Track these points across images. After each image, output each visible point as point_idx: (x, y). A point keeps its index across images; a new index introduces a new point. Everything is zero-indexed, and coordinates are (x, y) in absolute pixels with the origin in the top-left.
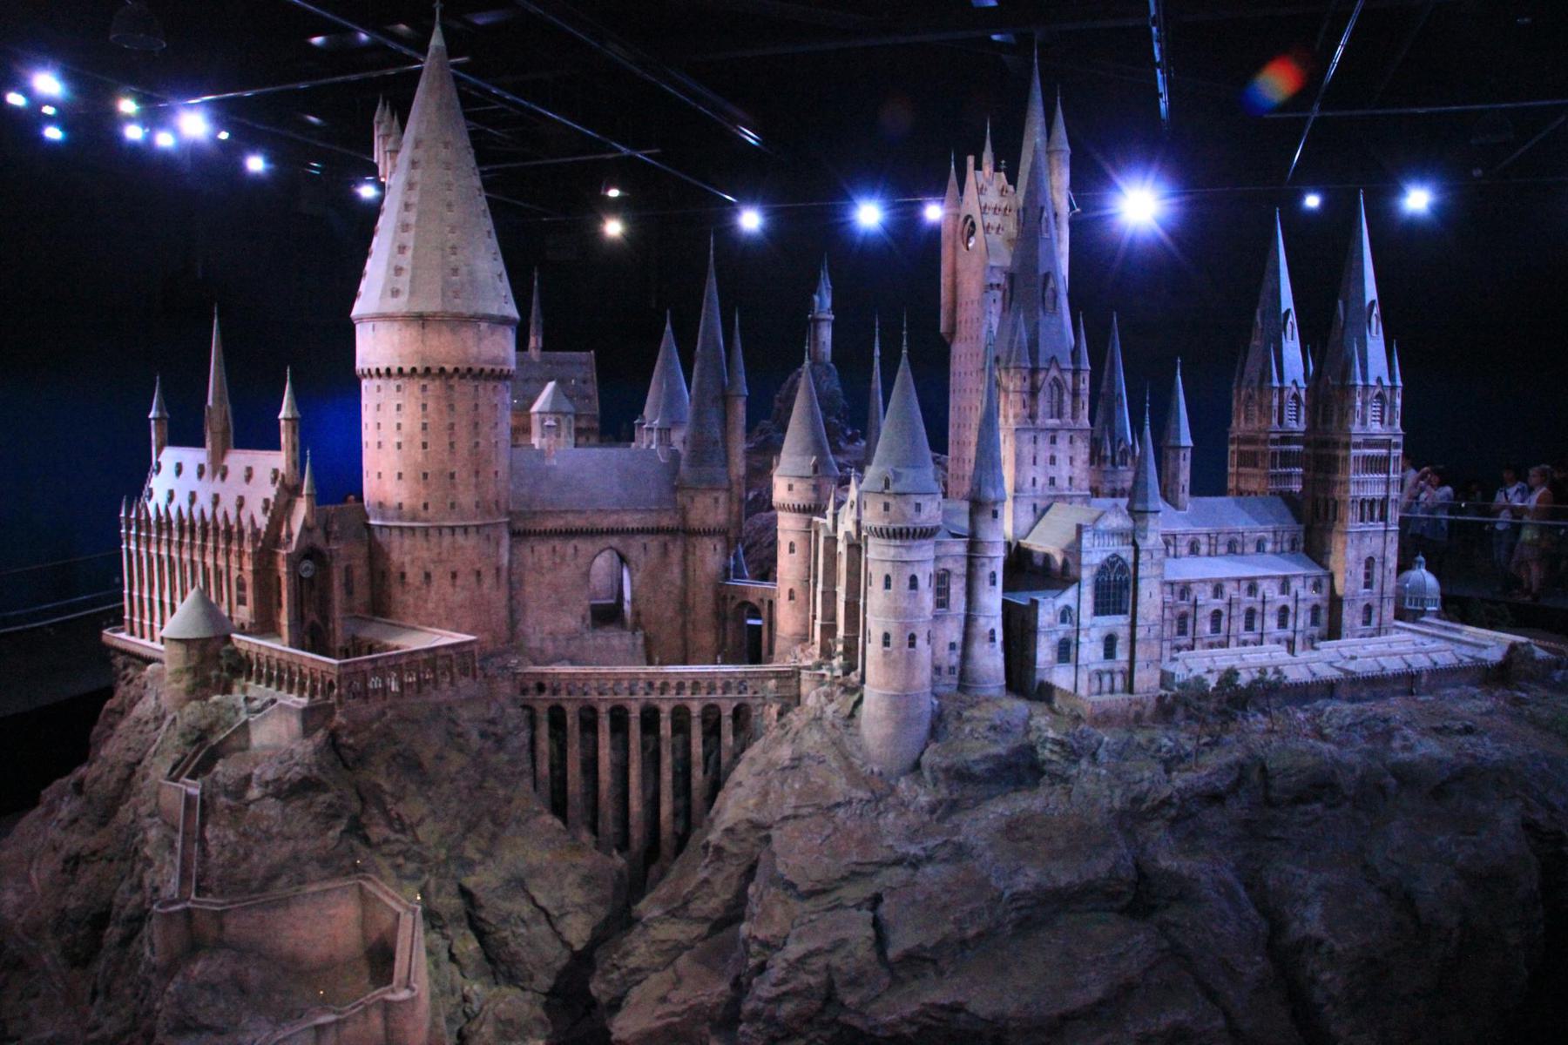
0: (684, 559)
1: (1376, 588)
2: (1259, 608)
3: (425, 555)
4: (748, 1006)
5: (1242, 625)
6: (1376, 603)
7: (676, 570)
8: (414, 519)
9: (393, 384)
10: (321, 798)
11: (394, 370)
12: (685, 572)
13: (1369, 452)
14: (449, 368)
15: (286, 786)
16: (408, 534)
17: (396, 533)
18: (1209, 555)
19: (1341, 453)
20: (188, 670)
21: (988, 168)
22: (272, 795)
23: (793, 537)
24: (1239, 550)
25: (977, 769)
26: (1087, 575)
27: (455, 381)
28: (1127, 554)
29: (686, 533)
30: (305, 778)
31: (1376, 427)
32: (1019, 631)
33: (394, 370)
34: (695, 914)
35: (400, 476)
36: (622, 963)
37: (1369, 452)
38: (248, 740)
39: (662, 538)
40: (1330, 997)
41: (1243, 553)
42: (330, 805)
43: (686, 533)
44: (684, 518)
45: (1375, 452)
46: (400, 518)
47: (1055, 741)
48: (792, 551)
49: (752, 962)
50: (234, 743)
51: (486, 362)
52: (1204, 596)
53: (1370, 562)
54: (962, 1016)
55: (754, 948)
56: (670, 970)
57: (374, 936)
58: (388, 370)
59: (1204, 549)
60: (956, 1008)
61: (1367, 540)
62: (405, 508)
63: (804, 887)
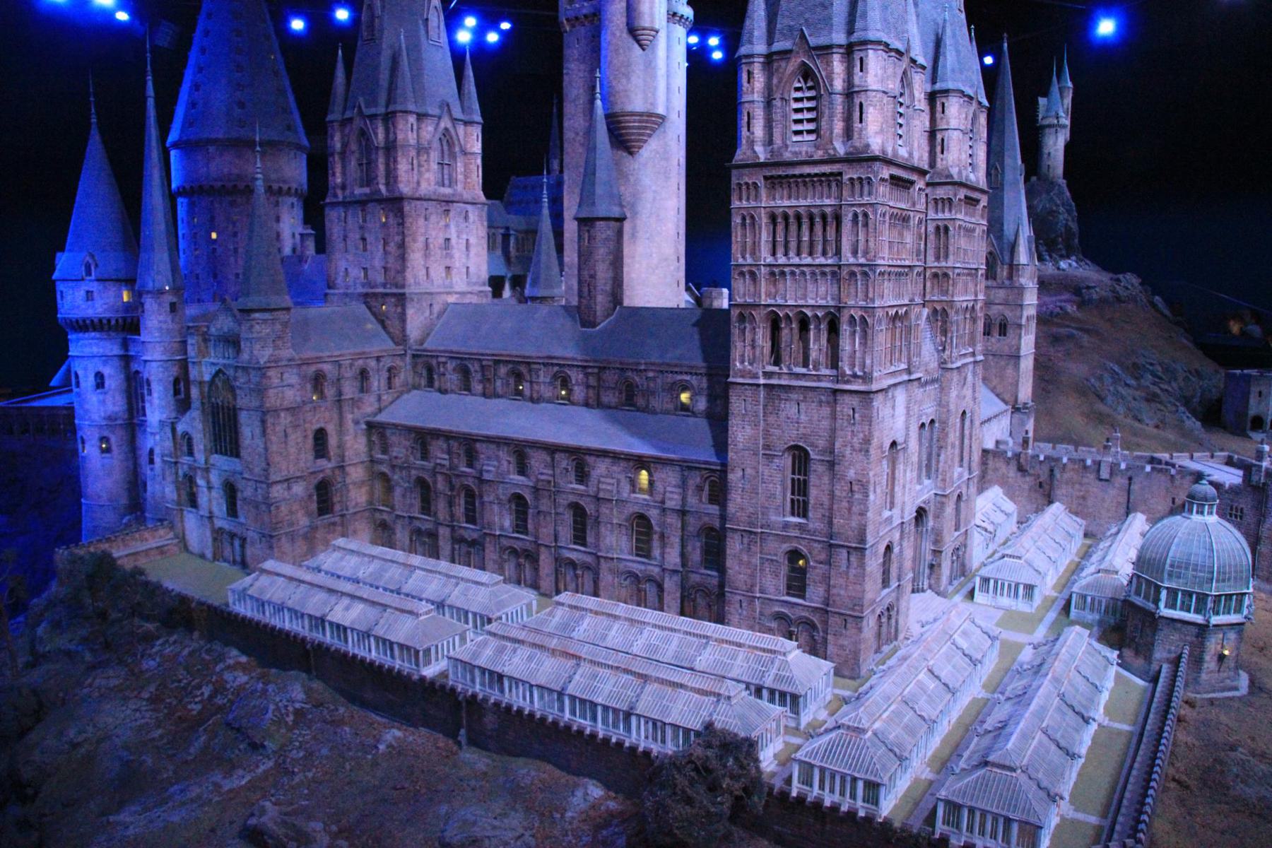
1: (815, 521)
2: (590, 509)
5: (566, 533)
6: (818, 552)
13: (784, 202)
18: (587, 405)
24: (641, 402)
31: (800, 146)
37: (784, 202)
41: (646, 410)
45: (804, 201)
51: (216, 180)
52: (497, 465)
53: (800, 457)
59: (579, 393)
61: (789, 409)
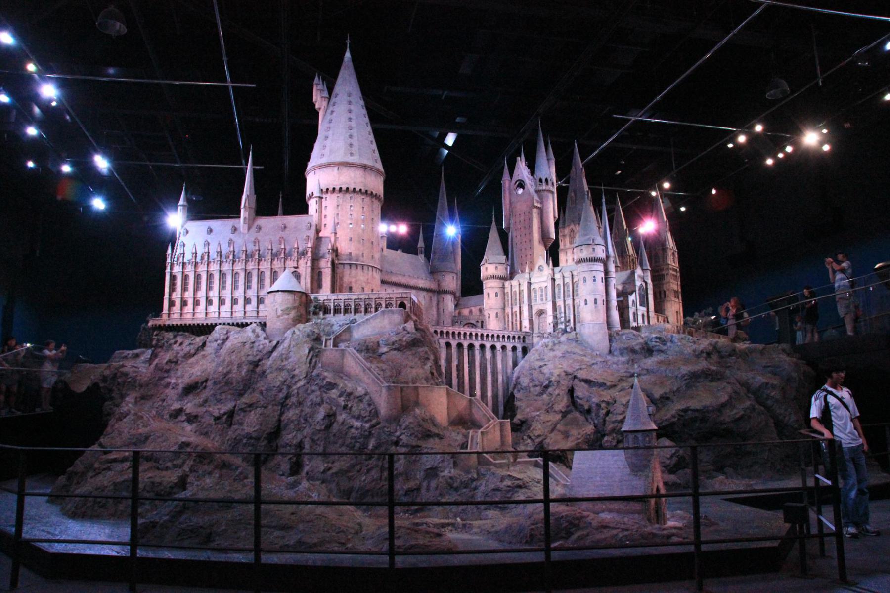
0: (438, 305)
3: (362, 278)
4: (609, 427)
7: (434, 309)
8: (357, 260)
9: (348, 196)
10: (421, 349)
11: (351, 189)
12: (438, 309)
14: (374, 193)
15: (404, 344)
16: (353, 267)
17: (347, 267)
19: (664, 272)
20: (294, 308)
21: (524, 164)
22: (395, 349)
23: (497, 290)
25: (637, 348)
26: (637, 289)
27: (374, 199)
28: (644, 284)
29: (439, 292)
30: (415, 339)
32: (623, 309)
33: (351, 189)
34: (557, 409)
35: (351, 239)
36: (531, 435)
38: (351, 336)
39: (430, 294)
40: (777, 401)
42: (426, 353)
43: (439, 292)
44: (439, 285)
46: (350, 260)
47: (657, 338)
48: (497, 296)
49: (604, 411)
50: (343, 337)
54: (690, 412)
55: (603, 405)
56: (555, 432)
57: (454, 414)
58: (347, 188)
60: (686, 410)
62: (353, 255)
63: (608, 384)
